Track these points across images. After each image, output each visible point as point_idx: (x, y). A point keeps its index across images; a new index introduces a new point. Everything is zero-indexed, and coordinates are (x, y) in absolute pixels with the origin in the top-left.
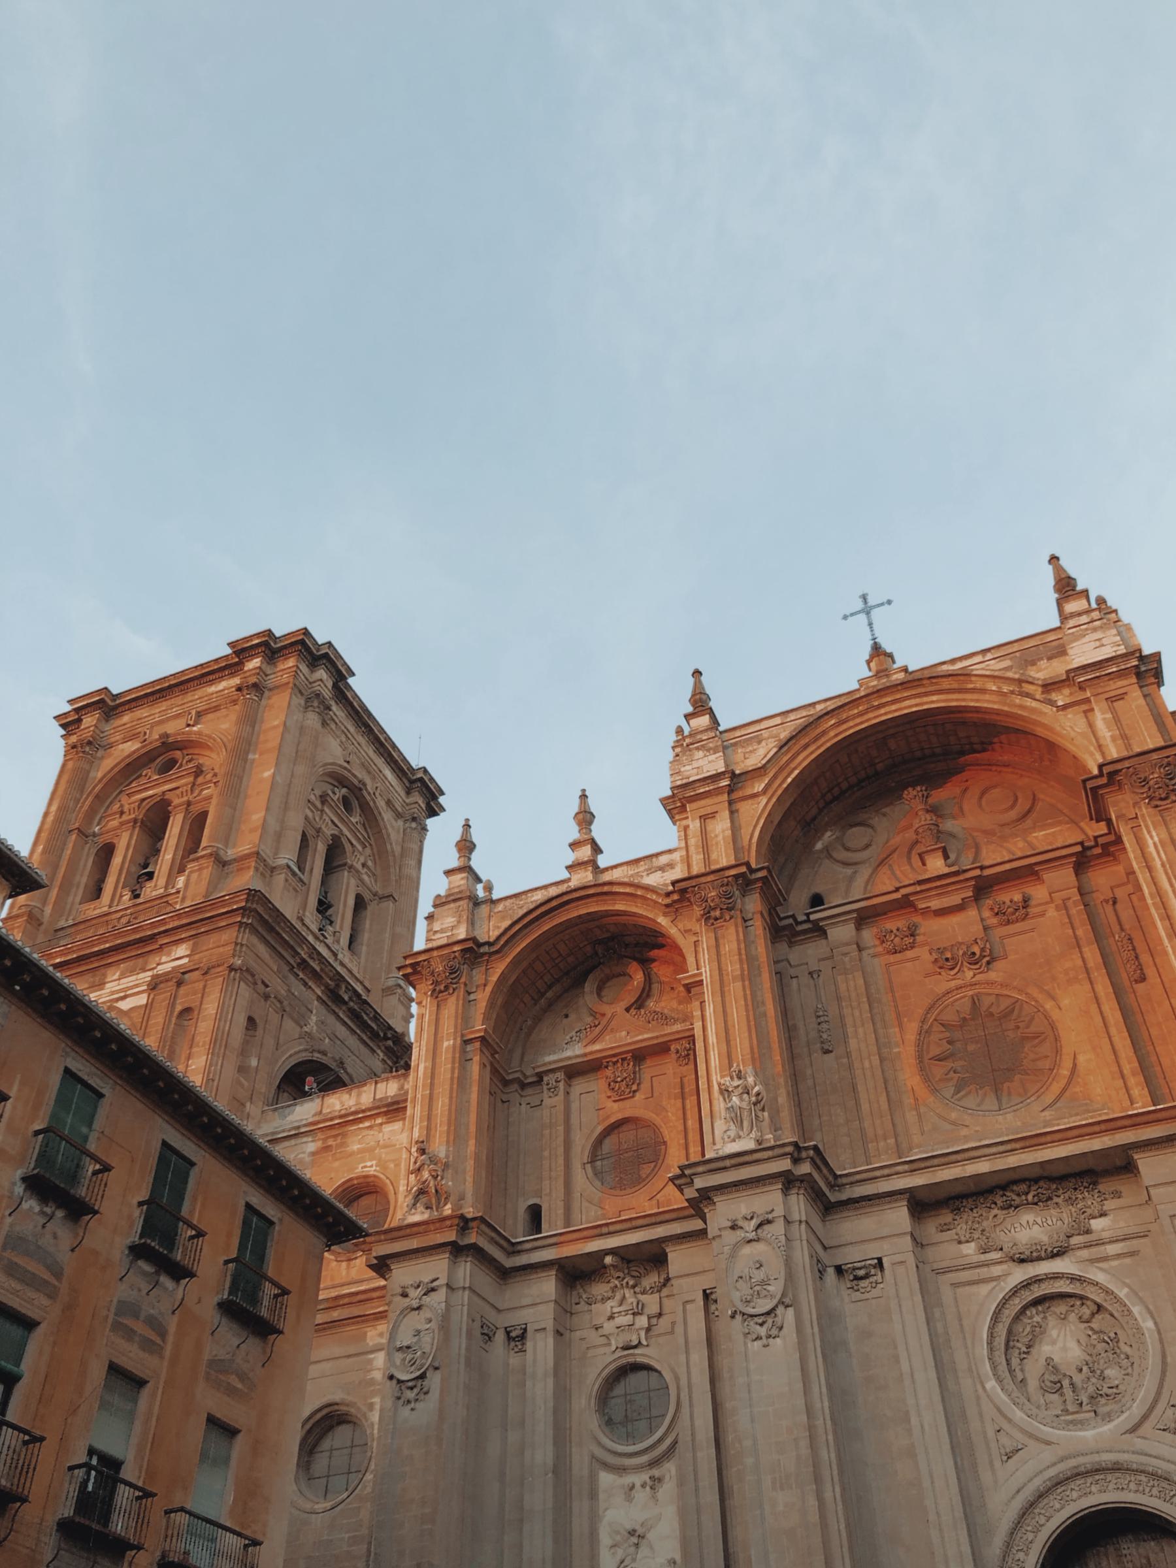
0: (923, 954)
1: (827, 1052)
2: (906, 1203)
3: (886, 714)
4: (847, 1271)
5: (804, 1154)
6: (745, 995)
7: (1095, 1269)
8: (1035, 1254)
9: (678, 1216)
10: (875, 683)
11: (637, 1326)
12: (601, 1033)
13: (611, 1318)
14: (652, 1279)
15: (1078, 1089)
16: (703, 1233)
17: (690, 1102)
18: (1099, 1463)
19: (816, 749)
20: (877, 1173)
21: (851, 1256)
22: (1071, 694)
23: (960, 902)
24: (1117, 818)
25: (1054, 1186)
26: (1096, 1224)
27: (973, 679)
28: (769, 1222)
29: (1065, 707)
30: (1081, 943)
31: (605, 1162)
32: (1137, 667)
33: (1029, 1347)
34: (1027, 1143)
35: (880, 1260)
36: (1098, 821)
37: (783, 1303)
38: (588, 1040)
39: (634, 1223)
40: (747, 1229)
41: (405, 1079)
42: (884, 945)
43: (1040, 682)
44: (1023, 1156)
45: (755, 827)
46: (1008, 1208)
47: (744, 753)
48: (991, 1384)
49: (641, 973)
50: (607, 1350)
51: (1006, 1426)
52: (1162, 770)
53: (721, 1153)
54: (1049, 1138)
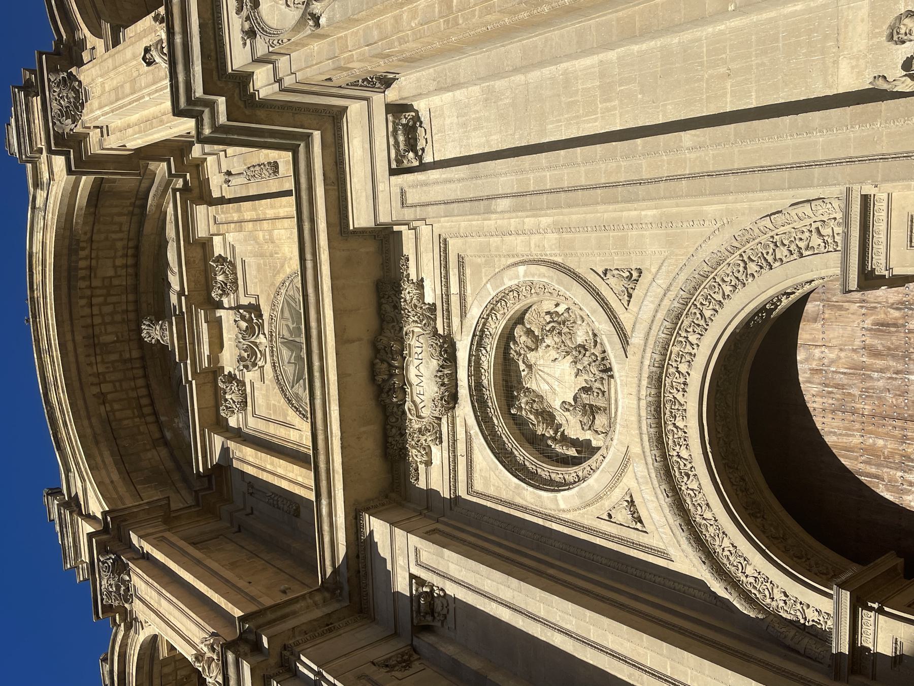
0: (250, 376)
1: (297, 514)
2: (367, 516)
3: (54, 340)
5: (252, 637)
7: (470, 313)
8: (446, 381)
18: (649, 404)
19: (69, 416)
20: (327, 539)
22: (44, 164)
23: (206, 324)
24: (104, 149)
25: (388, 333)
27: (34, 251)
30: (242, 218)
32: (26, 96)
35: (412, 576)
36: (138, 168)
42: (236, 411)
44: (330, 361)
46: (405, 392)
51: (607, 504)
54: (313, 324)
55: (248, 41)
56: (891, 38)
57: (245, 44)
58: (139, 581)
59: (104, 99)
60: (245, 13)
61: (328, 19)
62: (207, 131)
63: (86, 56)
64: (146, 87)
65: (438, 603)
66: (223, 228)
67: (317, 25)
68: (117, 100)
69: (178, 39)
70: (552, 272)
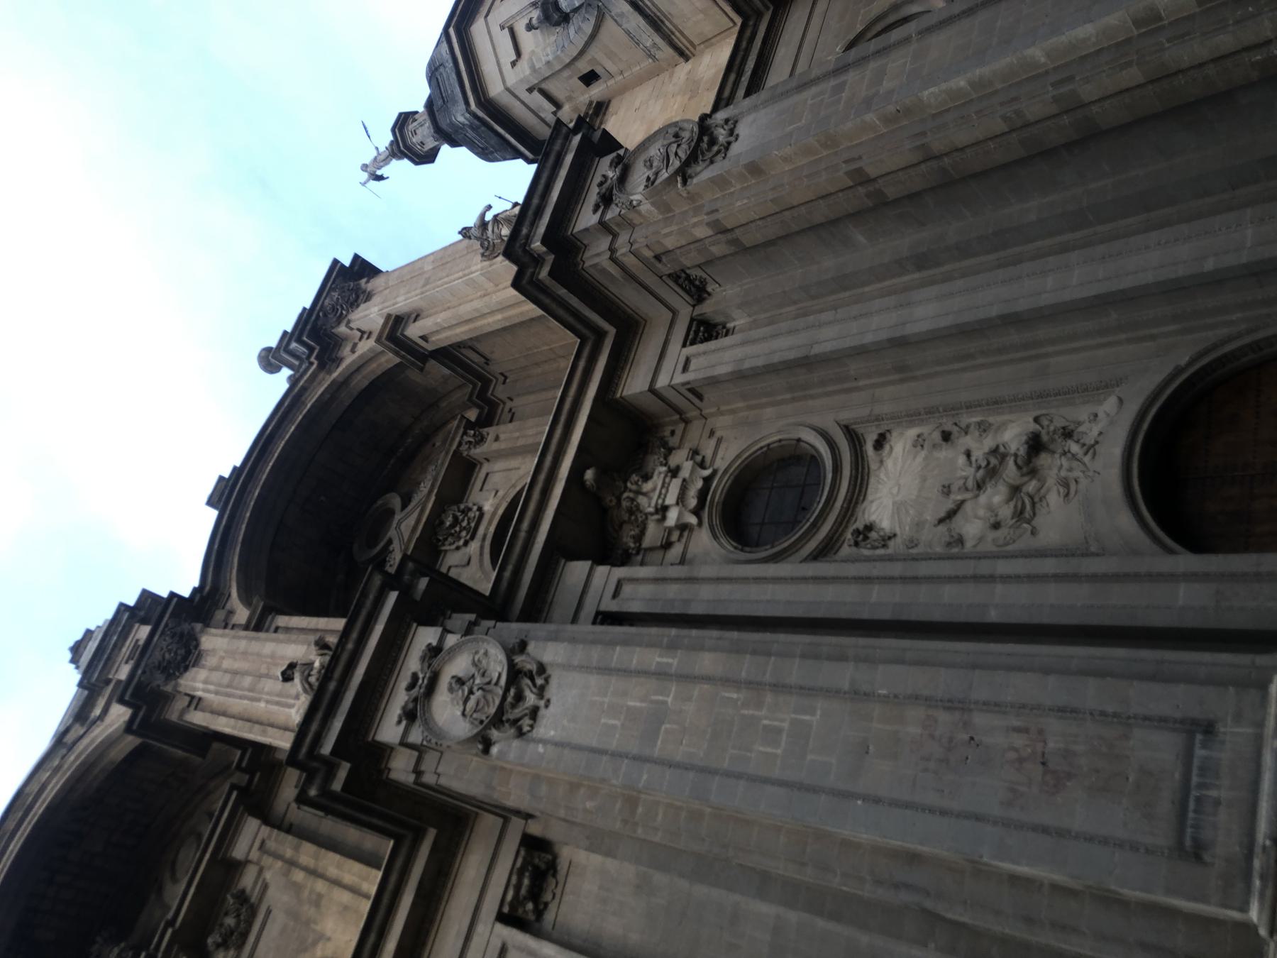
27: (28, 789)
52: (167, 638)
55: (404, 723)
57: (399, 722)
60: (415, 692)
61: (500, 752)
62: (313, 792)
63: (220, 615)
64: (268, 694)
66: (267, 860)
67: (486, 751)
68: (228, 686)
69: (332, 686)
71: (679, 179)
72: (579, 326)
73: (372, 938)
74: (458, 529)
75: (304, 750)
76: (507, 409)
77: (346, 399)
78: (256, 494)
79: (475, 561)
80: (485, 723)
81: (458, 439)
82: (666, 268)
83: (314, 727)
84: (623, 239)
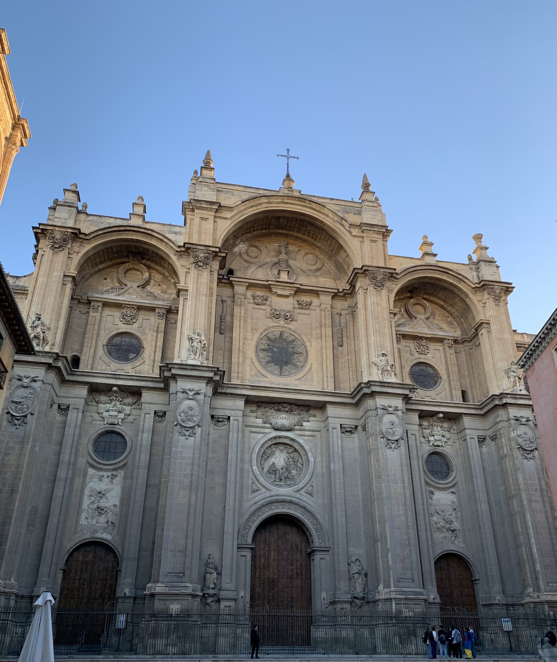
3: (288, 207)
4: (215, 418)
5: (219, 373)
6: (206, 303)
9: (153, 379)
10: (287, 192)
11: (119, 417)
12: (124, 293)
13: (108, 411)
14: (129, 400)
15: (309, 377)
16: (166, 389)
17: (161, 336)
20: (238, 386)
21: (219, 413)
22: (358, 232)
25: (296, 408)
26: (305, 424)
27: (325, 209)
28: (199, 394)
29: (355, 236)
31: (113, 347)
33: (268, 457)
34: (295, 391)
35: (229, 418)
37: (198, 425)
38: (118, 293)
39: (132, 378)
40: (190, 394)
41: (17, 279)
43: (349, 223)
45: (223, 232)
47: (225, 197)
48: (255, 468)
49: (148, 273)
50: (102, 423)
53: (184, 362)
54: (303, 392)
56: (358, 559)
58: (205, 274)
59: (376, 306)
65: (219, 424)
67: (381, 438)
68: (375, 317)
69: (387, 385)
70: (312, 470)
71: (519, 447)
72: (483, 405)
73: (330, 394)
74: (422, 347)
75: (372, 383)
76: (460, 349)
77: (463, 296)
78: (429, 275)
79: (413, 357)
80: (386, 436)
81: (450, 338)
82: (498, 434)
83: (377, 384)
84: (505, 424)
